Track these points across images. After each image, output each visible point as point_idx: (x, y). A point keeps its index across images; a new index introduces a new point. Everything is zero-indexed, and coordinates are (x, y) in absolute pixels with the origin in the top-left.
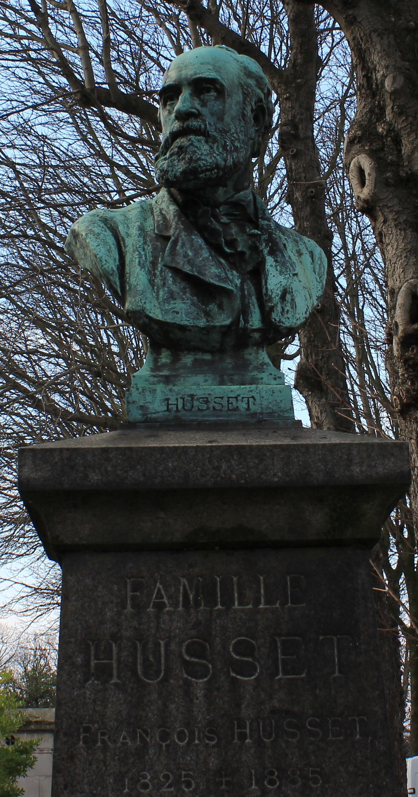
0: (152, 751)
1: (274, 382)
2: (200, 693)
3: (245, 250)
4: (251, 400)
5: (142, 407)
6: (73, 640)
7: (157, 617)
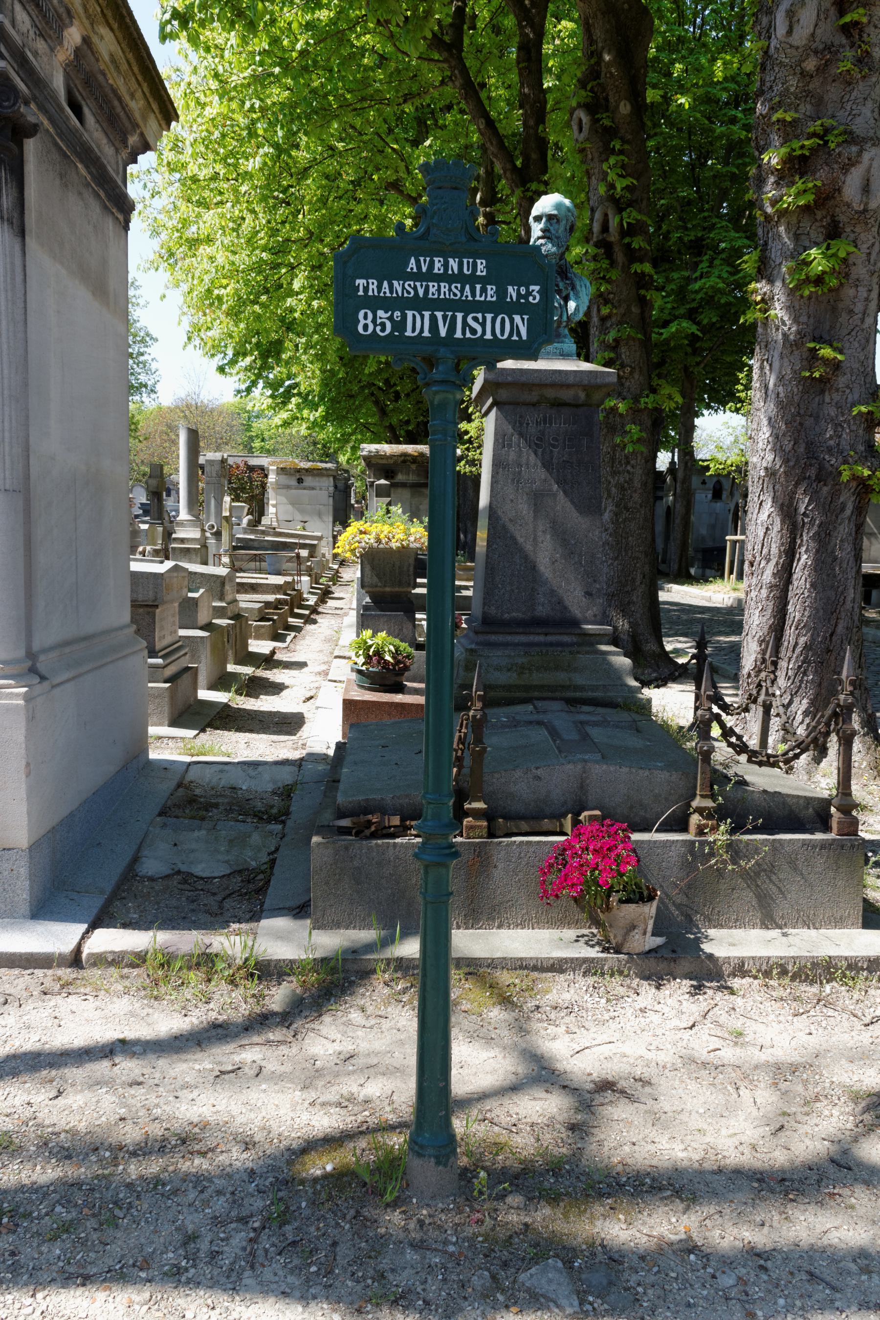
2: (540, 454)
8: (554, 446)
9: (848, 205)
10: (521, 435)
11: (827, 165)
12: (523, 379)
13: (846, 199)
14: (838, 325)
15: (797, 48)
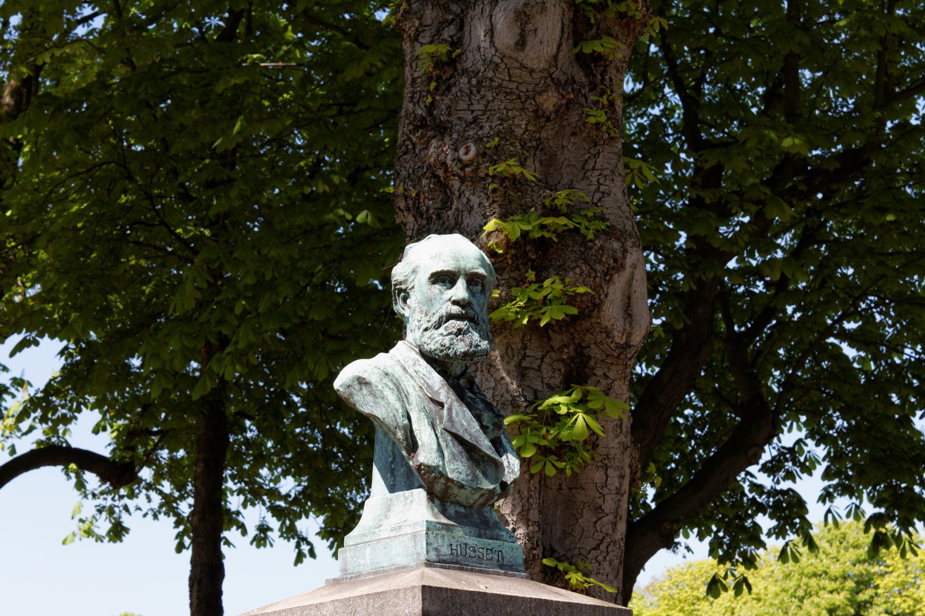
3: (489, 425)
5: (436, 549)
9: (608, 333)
11: (586, 262)
14: (578, 529)
15: (532, 71)
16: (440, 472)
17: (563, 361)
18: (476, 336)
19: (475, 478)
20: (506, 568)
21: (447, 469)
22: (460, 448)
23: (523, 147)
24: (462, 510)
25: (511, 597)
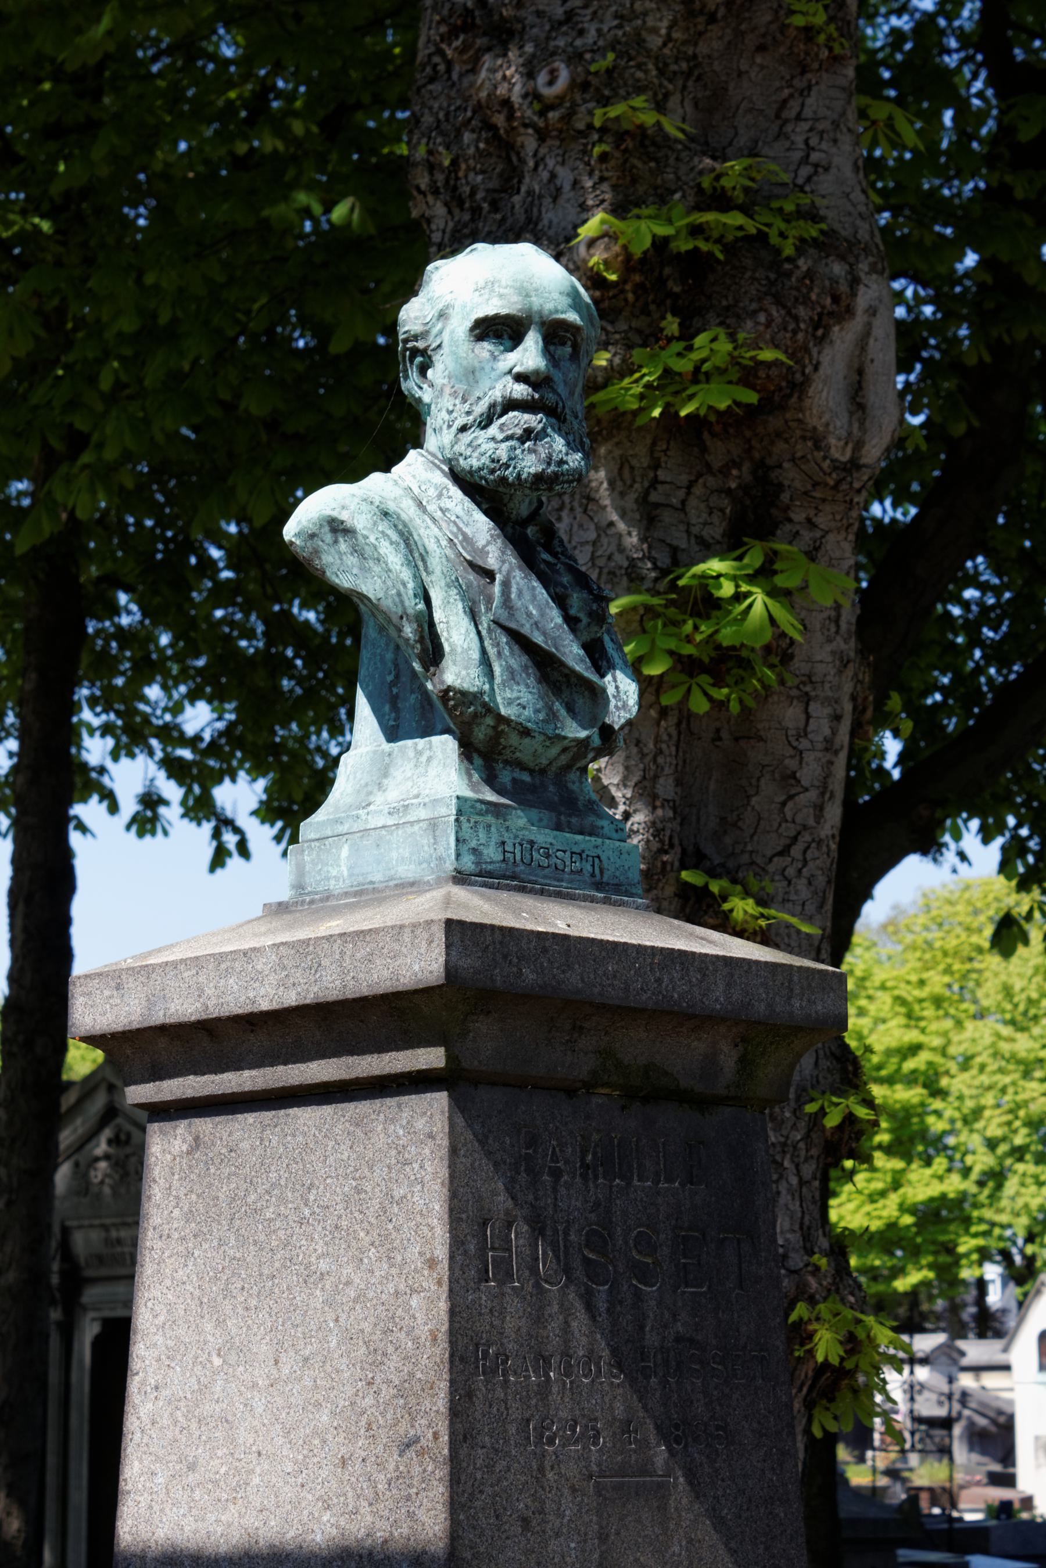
0: (555, 1389)
1: (614, 835)
2: (602, 1306)
3: (582, 615)
4: (597, 860)
6: (464, 1216)
7: (555, 1190)
8: (644, 1274)
9: (818, 441)
10: (538, 1227)
11: (779, 302)
12: (573, 979)
13: (813, 421)
16: (485, 705)
17: (729, 492)
18: (559, 443)
19: (552, 716)
20: (606, 889)
21: (499, 699)
22: (525, 659)
23: (661, 72)
24: (526, 777)
25: (615, 945)
